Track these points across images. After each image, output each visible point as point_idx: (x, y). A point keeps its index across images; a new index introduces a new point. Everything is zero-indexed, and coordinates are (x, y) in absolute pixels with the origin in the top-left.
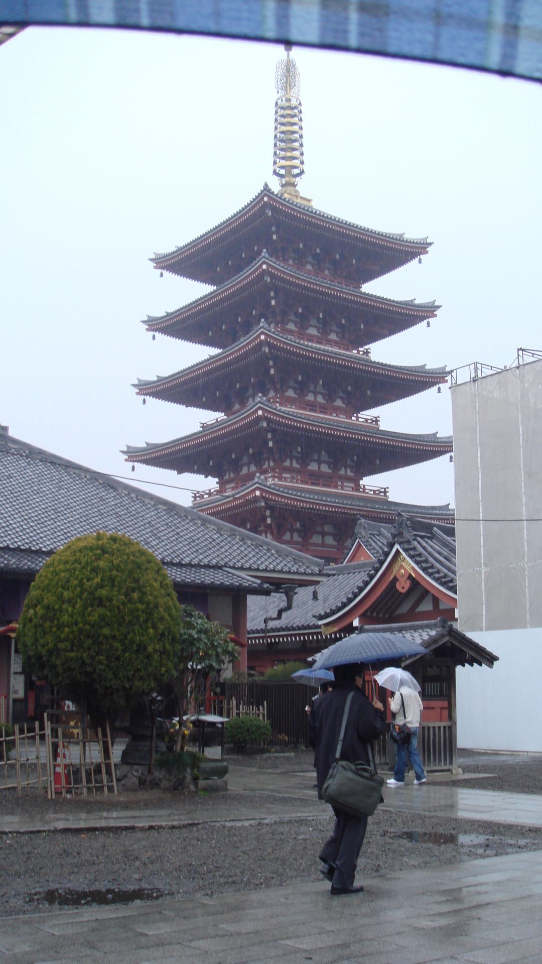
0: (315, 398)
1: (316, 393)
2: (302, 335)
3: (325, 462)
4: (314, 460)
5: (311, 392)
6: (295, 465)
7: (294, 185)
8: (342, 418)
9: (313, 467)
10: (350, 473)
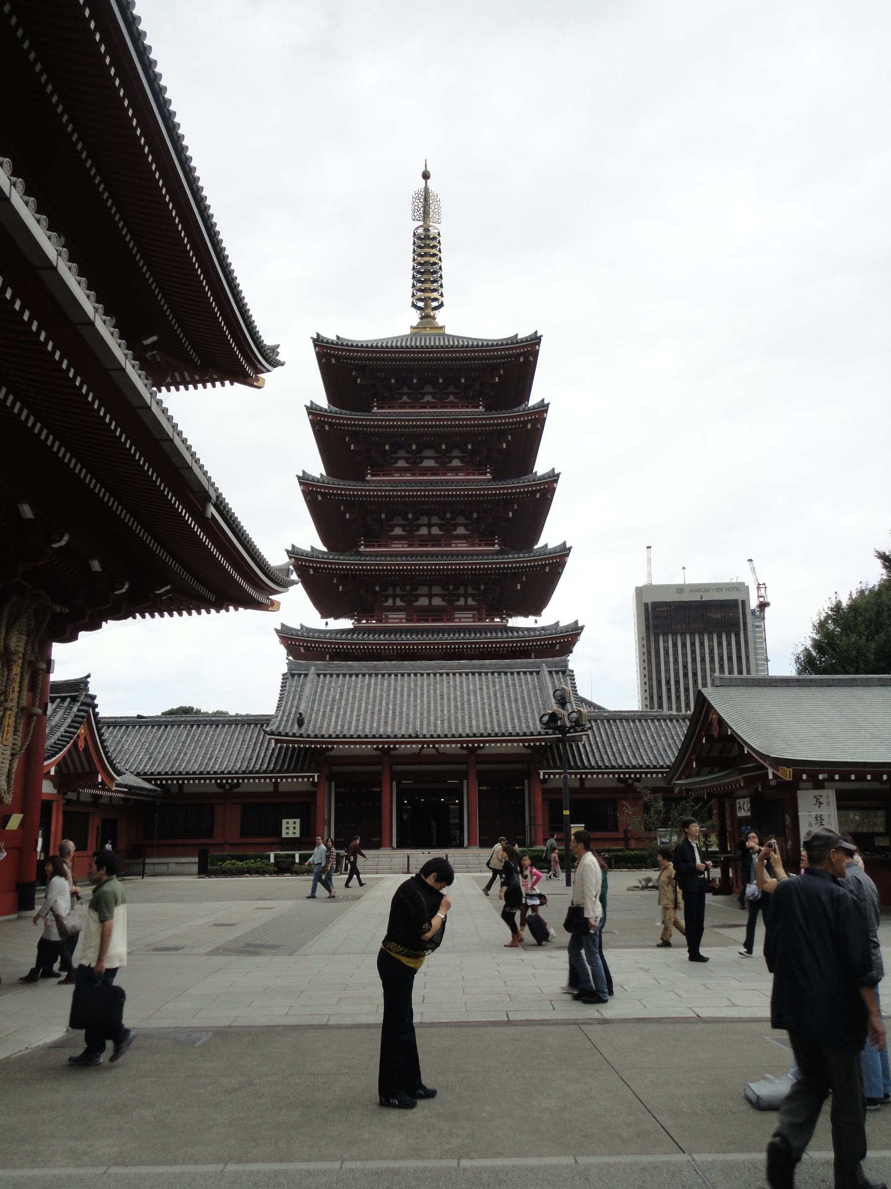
0: (429, 531)
1: (429, 526)
2: (414, 467)
3: (437, 595)
4: (423, 595)
5: (424, 525)
6: (399, 602)
7: (434, 318)
8: (463, 547)
9: (423, 602)
10: (470, 602)
